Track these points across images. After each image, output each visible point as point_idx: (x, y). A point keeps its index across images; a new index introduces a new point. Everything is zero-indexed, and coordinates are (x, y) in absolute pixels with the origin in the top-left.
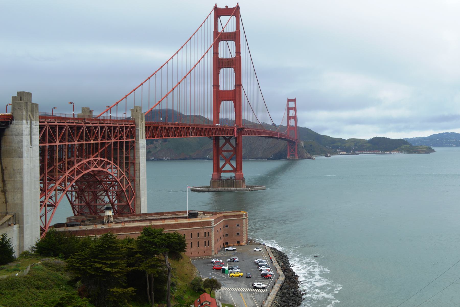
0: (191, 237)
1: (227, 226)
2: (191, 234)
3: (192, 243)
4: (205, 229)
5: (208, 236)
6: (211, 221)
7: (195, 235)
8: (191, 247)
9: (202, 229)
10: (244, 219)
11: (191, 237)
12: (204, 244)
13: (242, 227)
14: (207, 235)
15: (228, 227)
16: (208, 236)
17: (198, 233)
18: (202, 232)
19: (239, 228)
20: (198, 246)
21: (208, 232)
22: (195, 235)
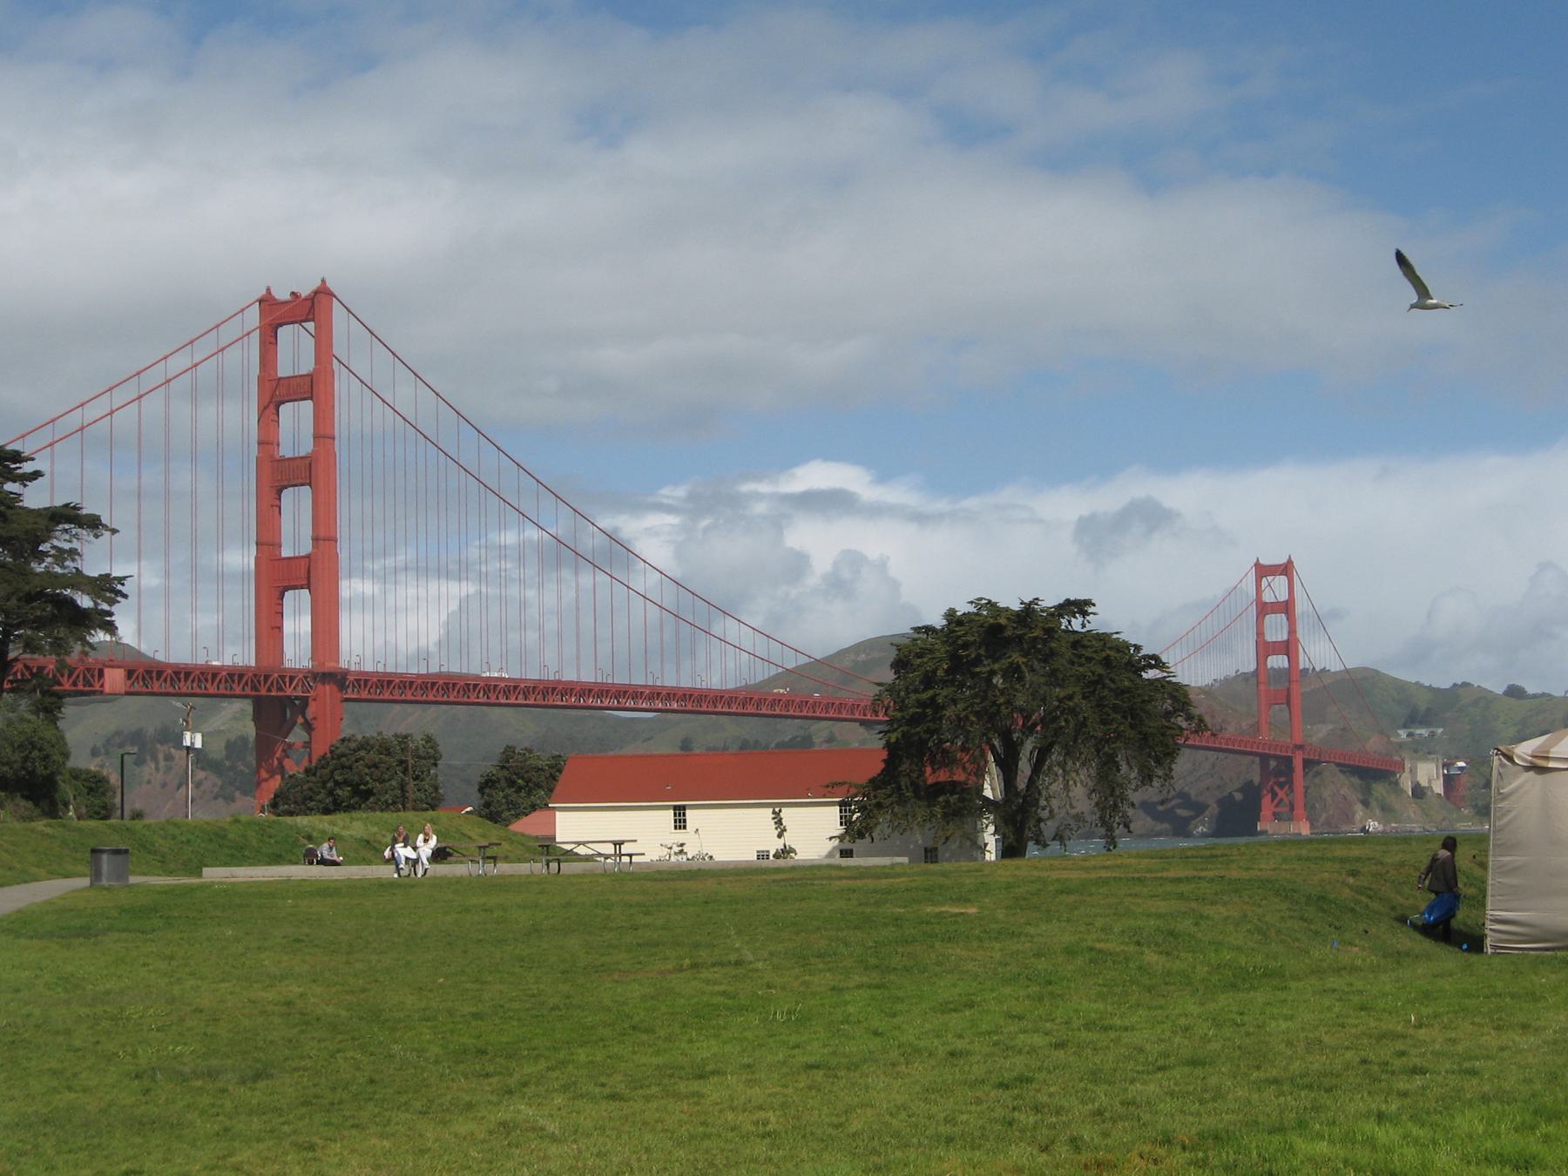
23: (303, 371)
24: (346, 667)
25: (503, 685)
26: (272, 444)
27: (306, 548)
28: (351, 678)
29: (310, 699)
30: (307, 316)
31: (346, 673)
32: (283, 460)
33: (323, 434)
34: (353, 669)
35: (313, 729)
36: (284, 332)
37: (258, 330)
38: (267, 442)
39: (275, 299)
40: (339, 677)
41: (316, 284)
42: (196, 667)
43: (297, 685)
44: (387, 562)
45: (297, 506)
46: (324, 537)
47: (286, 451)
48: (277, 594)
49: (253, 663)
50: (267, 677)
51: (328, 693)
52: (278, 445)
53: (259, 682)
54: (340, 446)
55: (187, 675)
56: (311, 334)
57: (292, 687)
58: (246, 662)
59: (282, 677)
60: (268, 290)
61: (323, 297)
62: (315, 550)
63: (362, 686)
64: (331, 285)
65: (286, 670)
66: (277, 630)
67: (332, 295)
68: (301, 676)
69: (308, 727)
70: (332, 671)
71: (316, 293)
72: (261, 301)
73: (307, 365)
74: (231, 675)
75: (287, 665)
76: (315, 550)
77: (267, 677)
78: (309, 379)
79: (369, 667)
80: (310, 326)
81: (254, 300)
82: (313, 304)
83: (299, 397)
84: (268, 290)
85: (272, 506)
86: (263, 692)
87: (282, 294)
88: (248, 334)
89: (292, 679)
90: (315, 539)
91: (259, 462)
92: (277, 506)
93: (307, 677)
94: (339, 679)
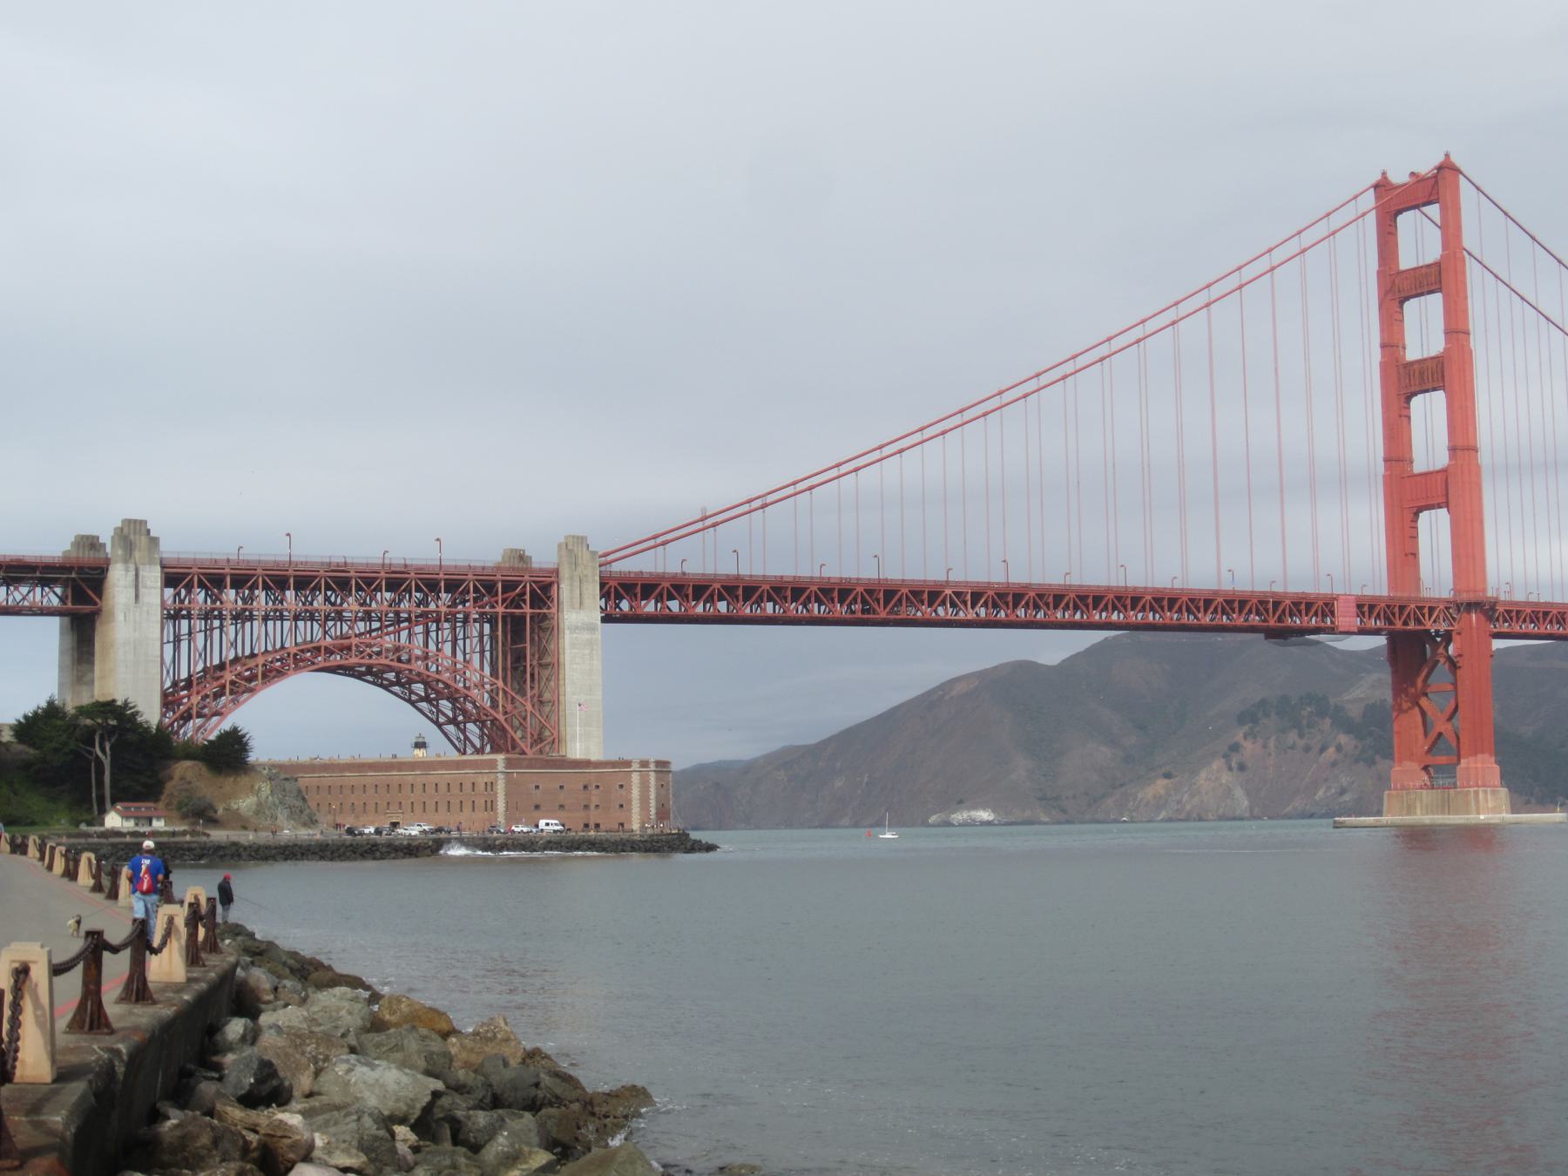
0: (461, 791)
1: (597, 787)
2: (461, 784)
3: (461, 802)
4: (486, 776)
5: (492, 790)
6: (496, 761)
7: (467, 787)
8: (461, 811)
9: (480, 775)
10: (634, 771)
11: (461, 791)
12: (483, 806)
13: (629, 791)
14: (489, 788)
15: (601, 788)
16: (492, 790)
17: (473, 784)
18: (481, 781)
19: (623, 792)
20: (473, 810)
21: (492, 783)
22: (467, 787)
23: (1430, 260)
24: (1495, 595)
26: (1398, 347)
27: (1441, 459)
28: (1501, 609)
29: (1454, 634)
30: (1430, 195)
31: (1493, 605)
32: (1412, 363)
33: (1456, 330)
34: (1502, 598)
35: (1460, 667)
36: (1406, 221)
37: (1374, 211)
38: (1391, 344)
40: (1487, 607)
41: (1441, 158)
42: (1318, 597)
43: (1438, 616)
45: (1429, 411)
46: (1463, 444)
47: (1412, 354)
48: (1409, 515)
50: (1402, 608)
52: (1404, 348)
53: (1394, 614)
54: (1477, 343)
55: (1309, 605)
56: (1436, 225)
57: (1432, 620)
58: (1378, 594)
59: (1421, 608)
60: (1384, 174)
61: (1447, 173)
62: (1453, 462)
63: (1514, 618)
64: (1457, 160)
65: (1424, 600)
66: (1411, 557)
67: (1458, 171)
68: (1442, 607)
69: (1453, 665)
70: (1480, 600)
71: (1440, 168)
72: (1376, 186)
75: (1425, 594)
76: (1453, 462)
77: (1402, 608)
78: (1437, 268)
79: (1519, 596)
80: (1434, 210)
82: (1436, 182)
83: (1426, 289)
84: (1384, 174)
85: (1400, 416)
86: (1399, 625)
87: (1399, 177)
88: (1364, 215)
89: (1431, 610)
90: (1453, 449)
91: (1384, 367)
92: (1406, 416)
93: (1449, 608)
94: (1488, 609)
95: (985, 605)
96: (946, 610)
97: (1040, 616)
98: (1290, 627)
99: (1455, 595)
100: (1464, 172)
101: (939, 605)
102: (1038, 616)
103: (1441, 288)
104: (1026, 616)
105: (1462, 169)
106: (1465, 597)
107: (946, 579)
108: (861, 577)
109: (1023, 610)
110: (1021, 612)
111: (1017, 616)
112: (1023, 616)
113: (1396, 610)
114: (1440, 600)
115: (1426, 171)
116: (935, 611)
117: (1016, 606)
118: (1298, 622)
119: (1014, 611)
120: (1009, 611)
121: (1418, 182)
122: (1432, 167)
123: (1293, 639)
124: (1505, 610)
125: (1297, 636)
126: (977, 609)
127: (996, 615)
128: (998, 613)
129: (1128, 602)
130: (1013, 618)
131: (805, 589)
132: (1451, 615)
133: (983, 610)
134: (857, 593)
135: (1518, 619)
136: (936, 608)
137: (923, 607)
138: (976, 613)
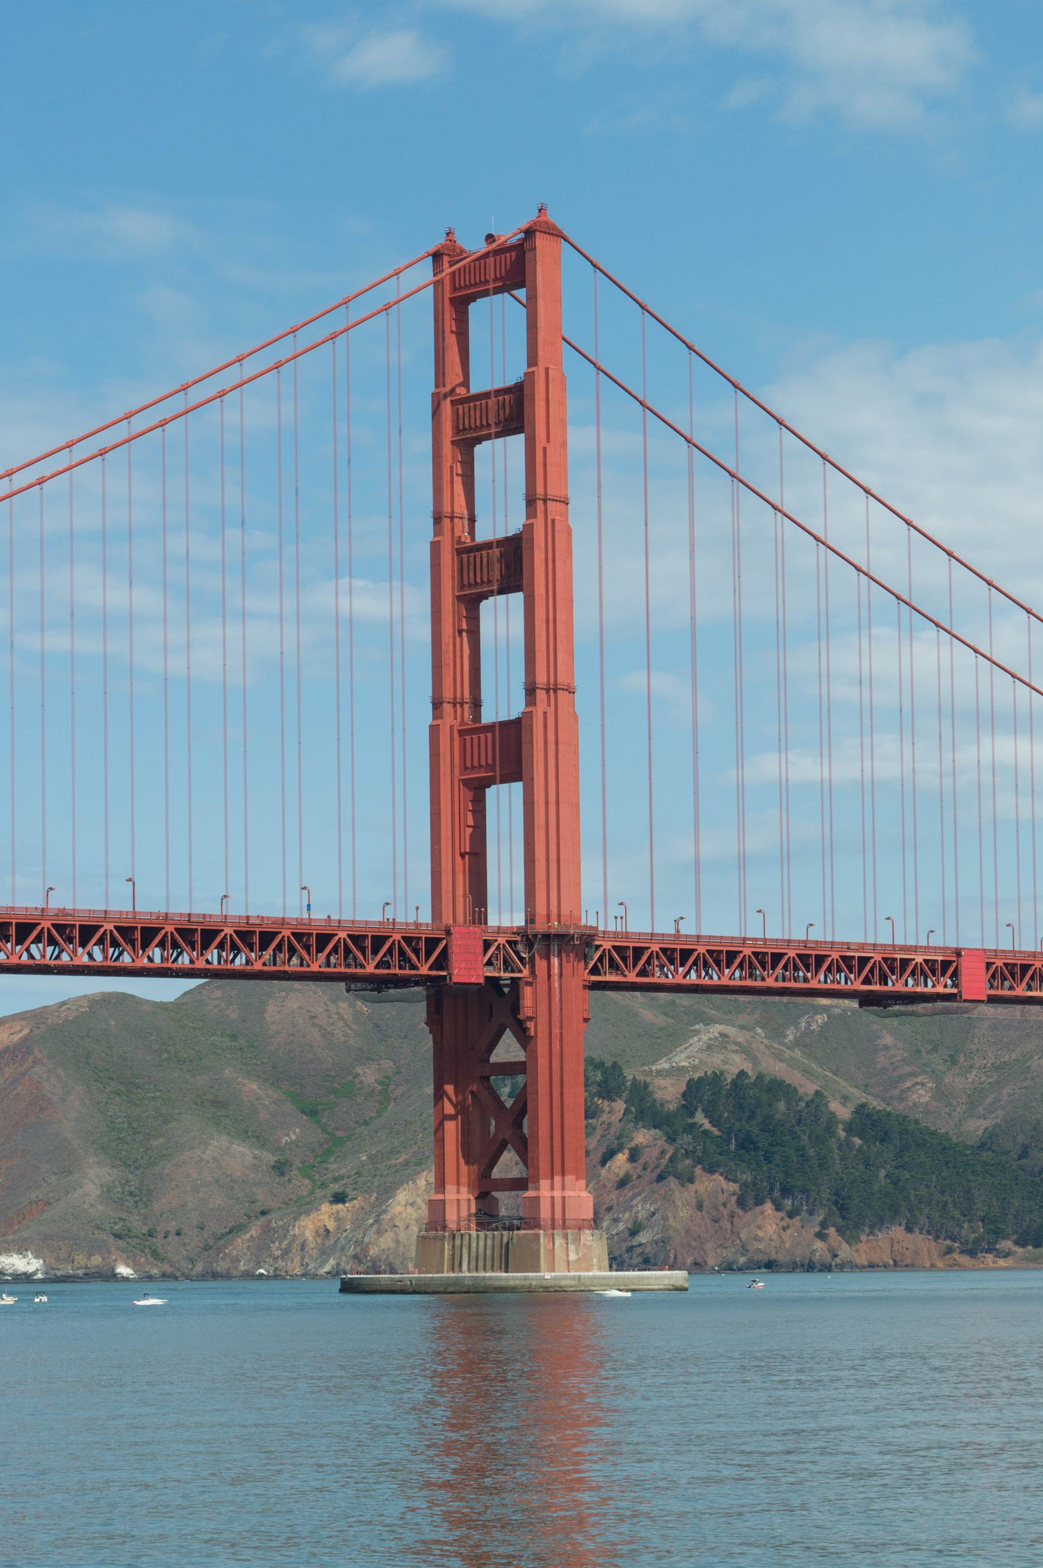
25: (919, 959)
28: (607, 945)
29: (521, 984)
39: (462, 251)
44: (540, 686)
49: (426, 917)
51: (556, 970)
64: (554, 217)
67: (560, 236)
68: (502, 940)
69: (525, 1038)
71: (529, 233)
73: (513, 372)
74: (357, 939)
81: (422, 254)
86: (424, 970)
87: (474, 244)
95: (162, 944)
96: (104, 951)
97: (240, 961)
98: (218, 970)
99: (530, 919)
100: (572, 239)
101: (32, 942)
102: (238, 961)
103: (523, 427)
104: (219, 962)
105: (566, 233)
106: (540, 927)
107: (40, 904)
108: (17, 905)
109: (215, 951)
110: (213, 955)
111: (207, 961)
112: (215, 962)
113: (422, 945)
114: (499, 930)
115: (508, 235)
116: (28, 950)
117: (205, 946)
118: (715, 977)
119: (202, 955)
120: (195, 953)
121: (497, 252)
122: (515, 231)
123: (897, 1008)
124: (614, 947)
125: (903, 1004)
126: (89, 947)
127: (117, 959)
128: (121, 954)
129: (313, 941)
130: (201, 964)
131: (275, 934)
132: (517, 953)
133: (157, 951)
134: (166, 935)
135: (903, 970)
136: (29, 946)
137: (9, 945)
138: (149, 957)
